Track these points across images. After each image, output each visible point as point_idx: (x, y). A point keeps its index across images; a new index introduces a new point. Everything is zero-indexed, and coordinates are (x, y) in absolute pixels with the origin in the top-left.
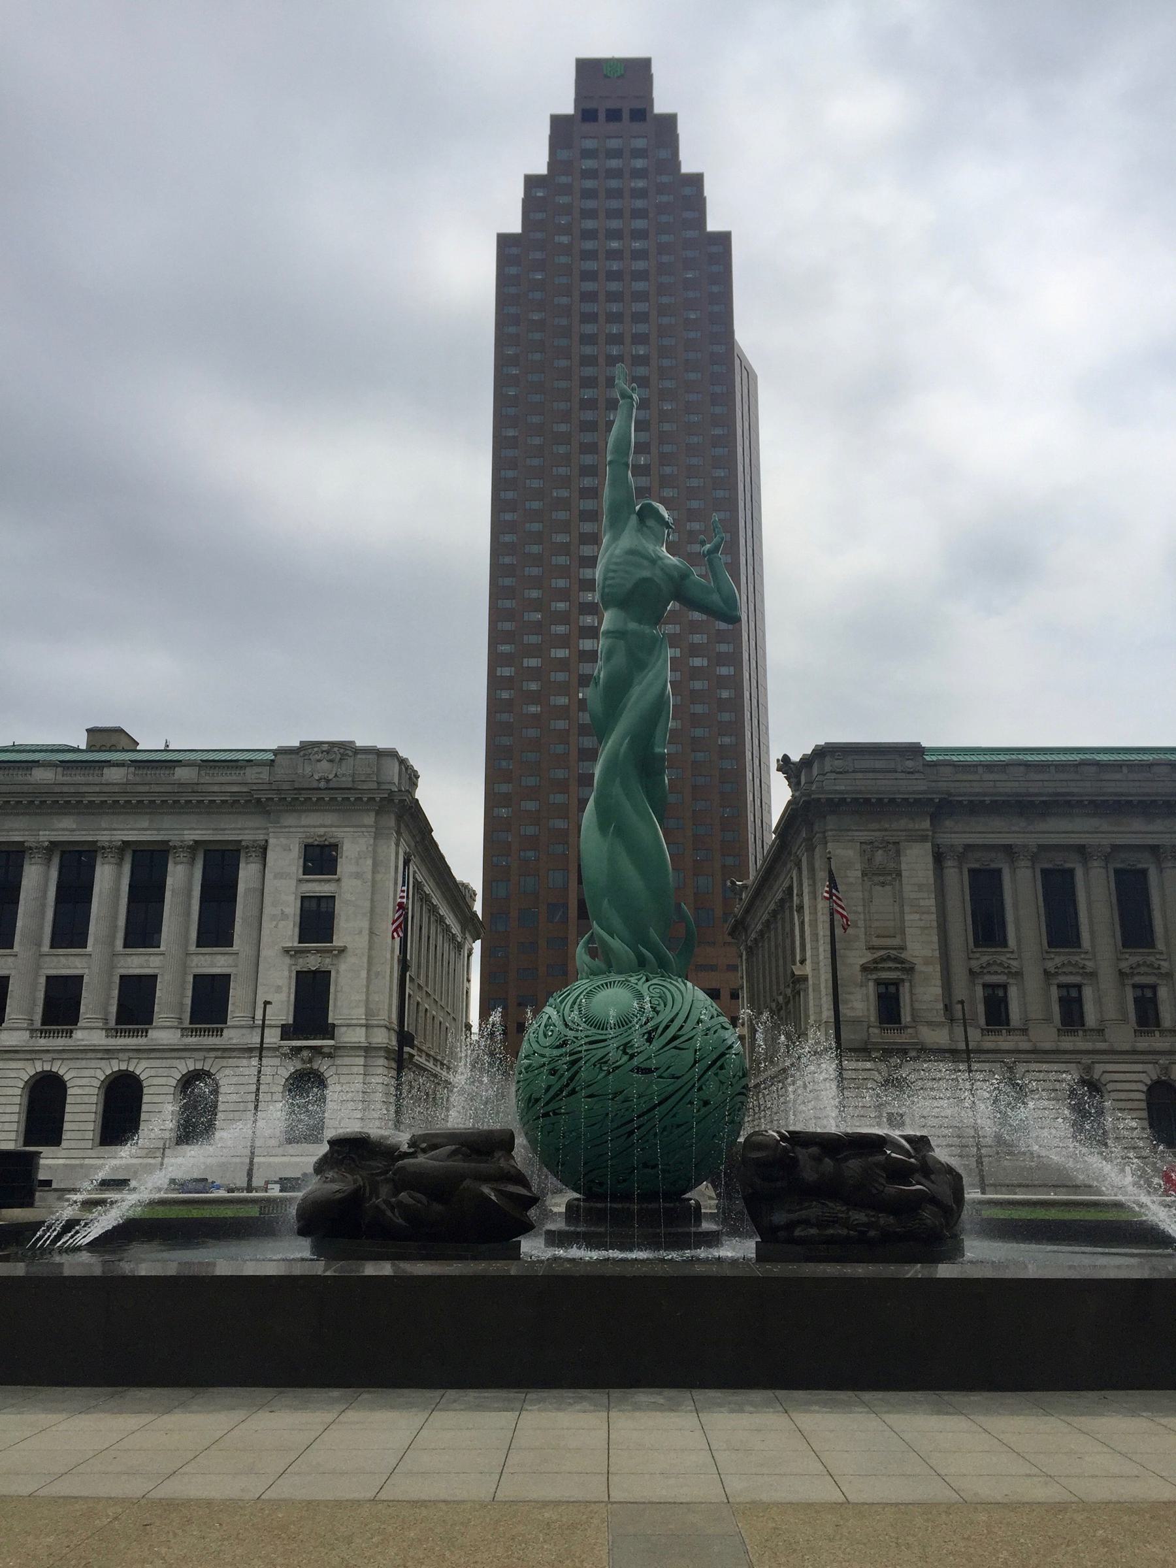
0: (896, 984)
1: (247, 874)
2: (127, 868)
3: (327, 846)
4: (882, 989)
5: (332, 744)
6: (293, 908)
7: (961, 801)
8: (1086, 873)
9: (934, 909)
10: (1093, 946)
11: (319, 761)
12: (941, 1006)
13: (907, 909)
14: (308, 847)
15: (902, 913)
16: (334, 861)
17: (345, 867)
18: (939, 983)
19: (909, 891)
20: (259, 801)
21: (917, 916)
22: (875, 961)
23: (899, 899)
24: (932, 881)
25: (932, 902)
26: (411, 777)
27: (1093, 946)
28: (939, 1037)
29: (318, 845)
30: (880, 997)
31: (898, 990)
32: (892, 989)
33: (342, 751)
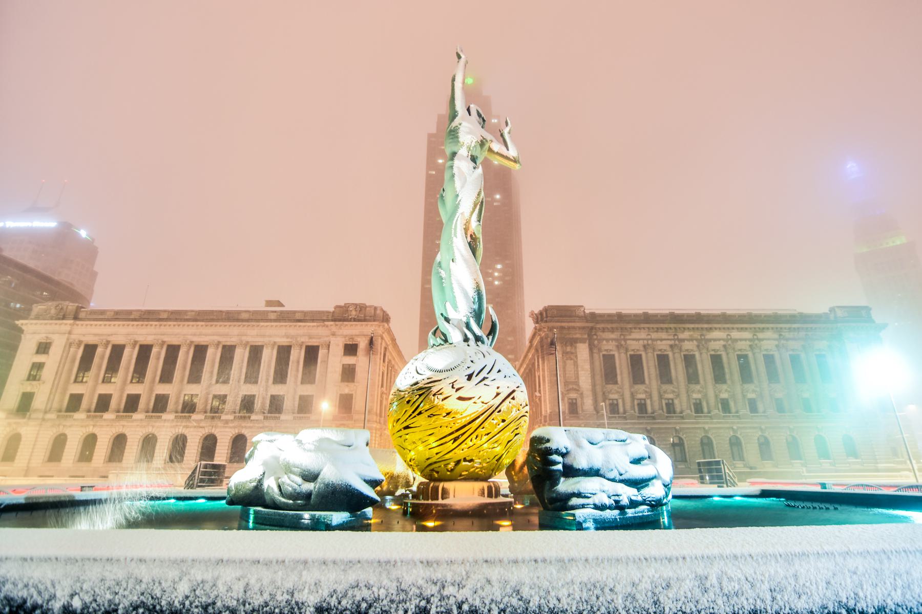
0: (576, 399)
1: (322, 353)
2: (275, 352)
4: (570, 401)
6: (339, 369)
7: (599, 328)
8: (647, 354)
9: (589, 370)
10: (650, 383)
12: (592, 408)
13: (579, 369)
15: (578, 371)
18: (591, 398)
19: (580, 362)
20: (327, 326)
21: (583, 372)
23: (576, 364)
24: (588, 358)
25: (589, 366)
27: (650, 383)
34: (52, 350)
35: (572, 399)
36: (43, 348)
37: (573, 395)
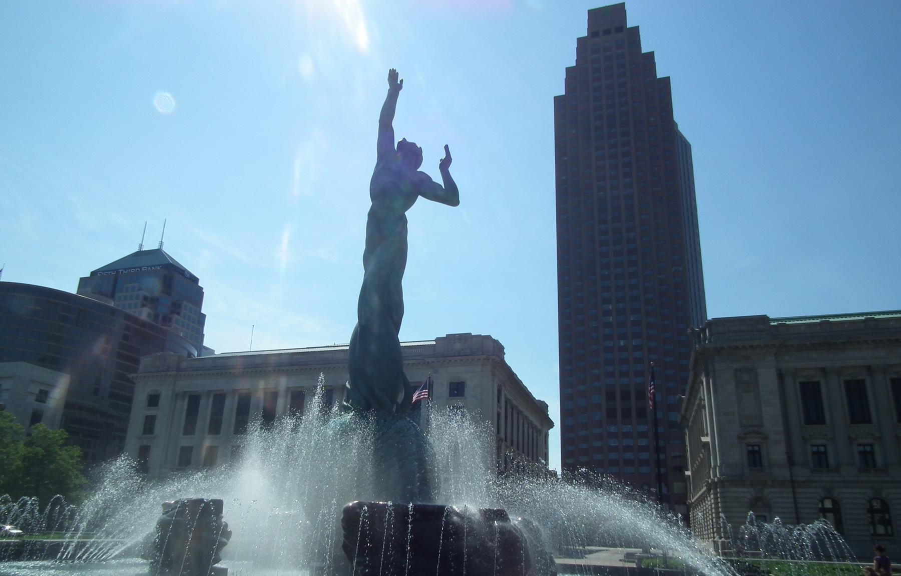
0: (759, 446)
3: (459, 383)
4: (750, 448)
5: (460, 335)
11: (455, 343)
12: (785, 457)
14: (451, 384)
16: (463, 389)
17: (468, 392)
20: (428, 363)
22: (745, 434)
26: (498, 349)
28: (785, 473)
29: (456, 383)
30: (749, 452)
31: (759, 448)
32: (756, 448)
33: (465, 338)
34: (162, 402)
35: (753, 446)
36: (153, 400)
37: (754, 440)
